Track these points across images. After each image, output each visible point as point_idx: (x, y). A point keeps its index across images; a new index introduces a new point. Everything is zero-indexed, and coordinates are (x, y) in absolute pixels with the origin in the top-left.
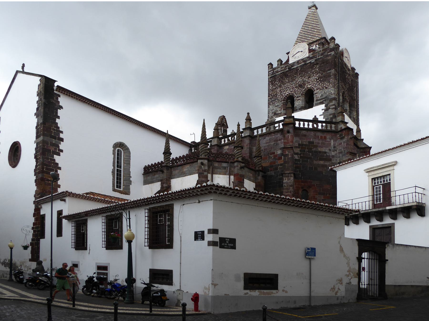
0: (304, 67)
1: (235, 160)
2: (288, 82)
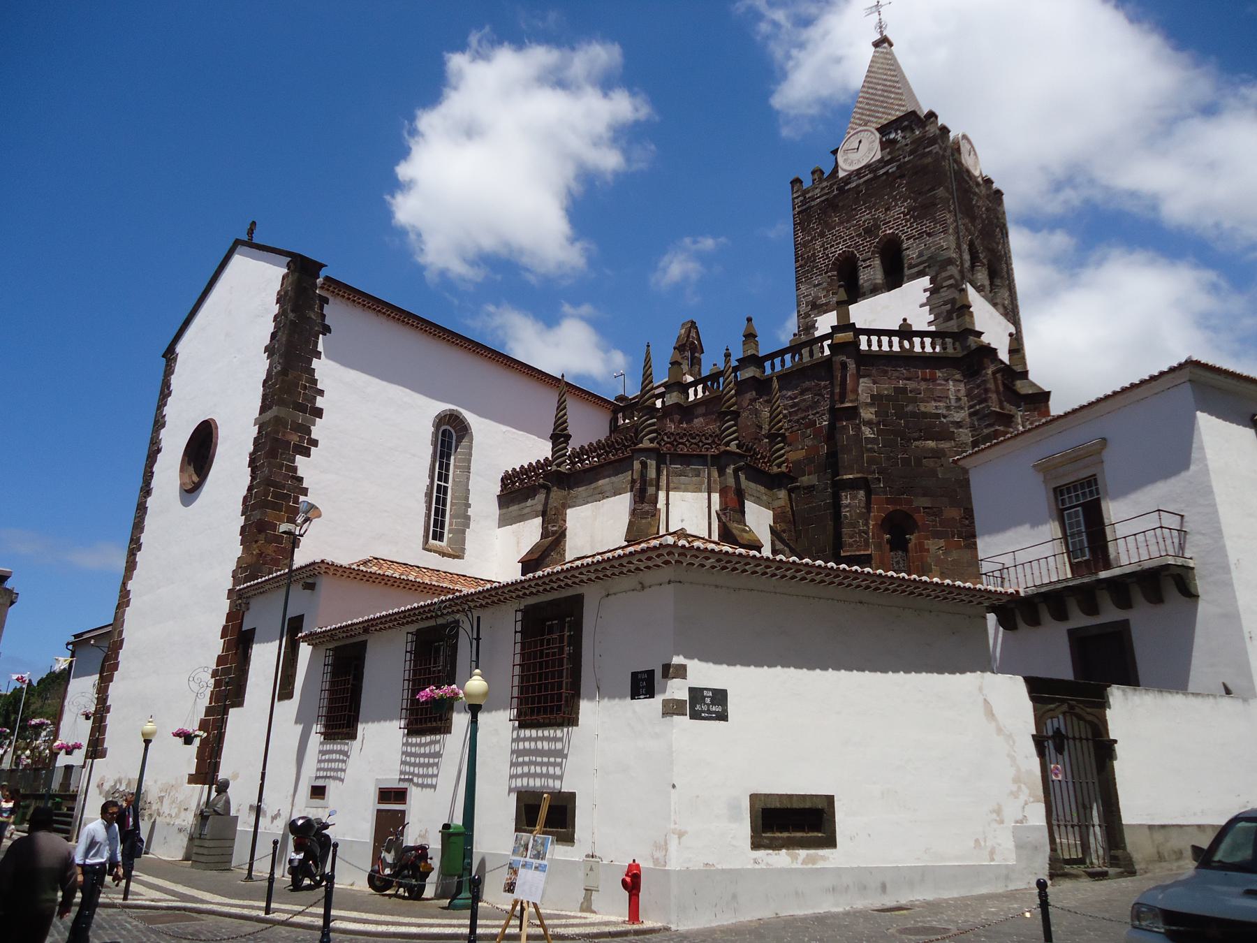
1: (722, 448)
2: (841, 223)
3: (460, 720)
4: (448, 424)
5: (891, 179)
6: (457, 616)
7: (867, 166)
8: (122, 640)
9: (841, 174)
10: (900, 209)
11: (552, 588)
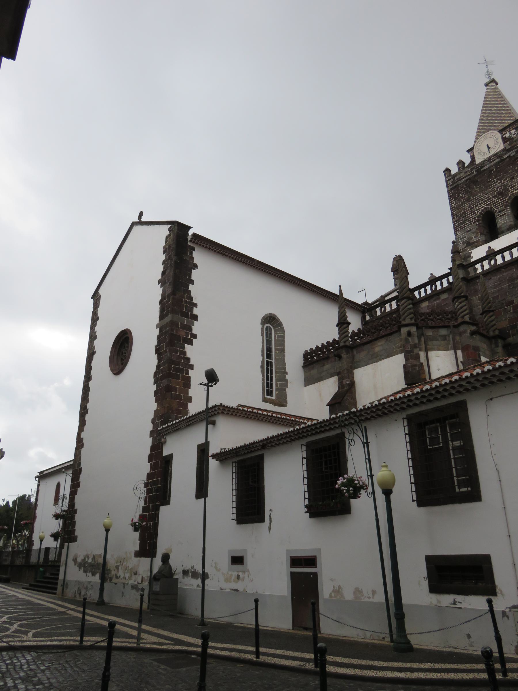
1: (460, 320)
2: (481, 191)
3: (361, 505)
5: (512, 161)
6: (344, 430)
7: (496, 155)
8: (81, 469)
9: (478, 161)
11: (335, 427)
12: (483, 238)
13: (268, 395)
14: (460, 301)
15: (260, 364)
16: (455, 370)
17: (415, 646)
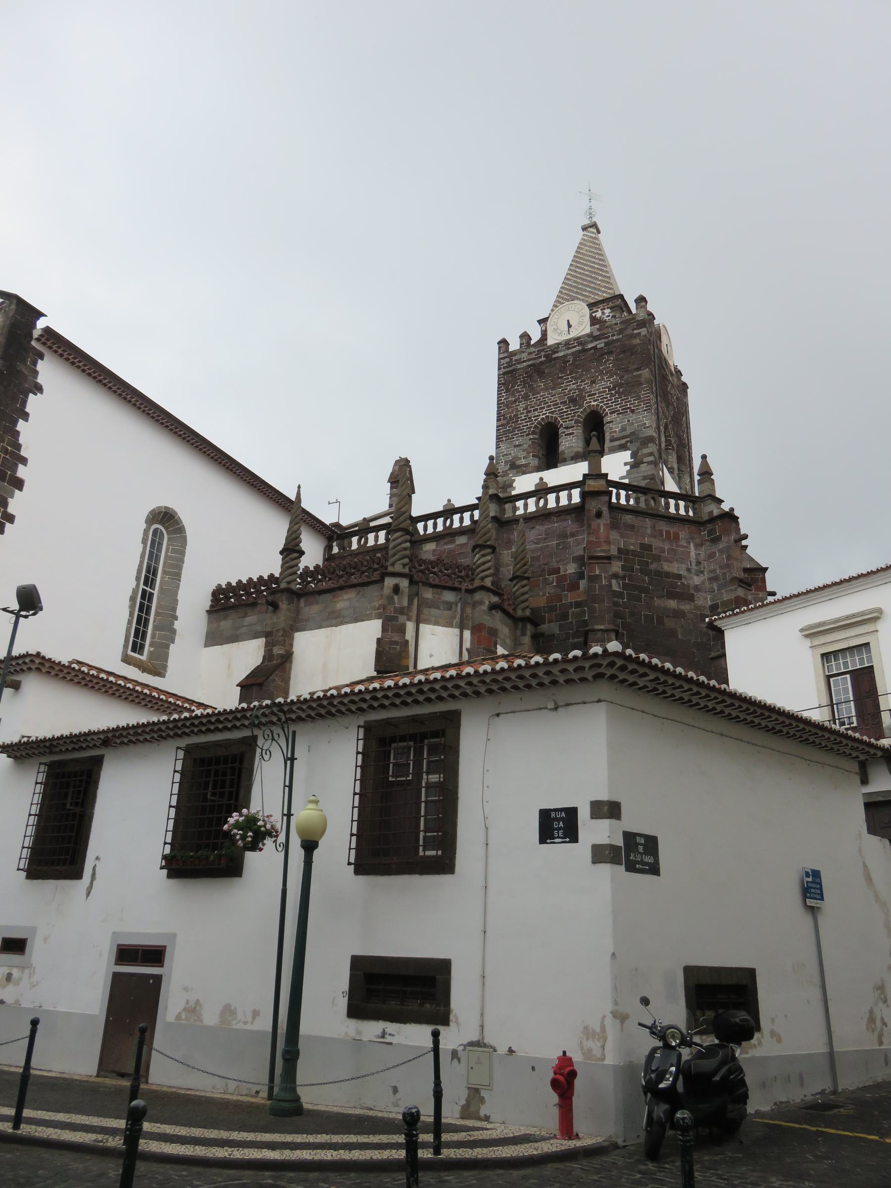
0: (579, 357)
1: (477, 583)
2: (546, 389)
3: (263, 864)
4: (161, 522)
5: (599, 355)
6: (256, 732)
7: (577, 339)
9: (550, 341)
10: (604, 383)
11: (243, 725)
12: (536, 462)
13: (134, 650)
14: (483, 552)
15: (130, 593)
16: (455, 660)
17: (306, 1106)
